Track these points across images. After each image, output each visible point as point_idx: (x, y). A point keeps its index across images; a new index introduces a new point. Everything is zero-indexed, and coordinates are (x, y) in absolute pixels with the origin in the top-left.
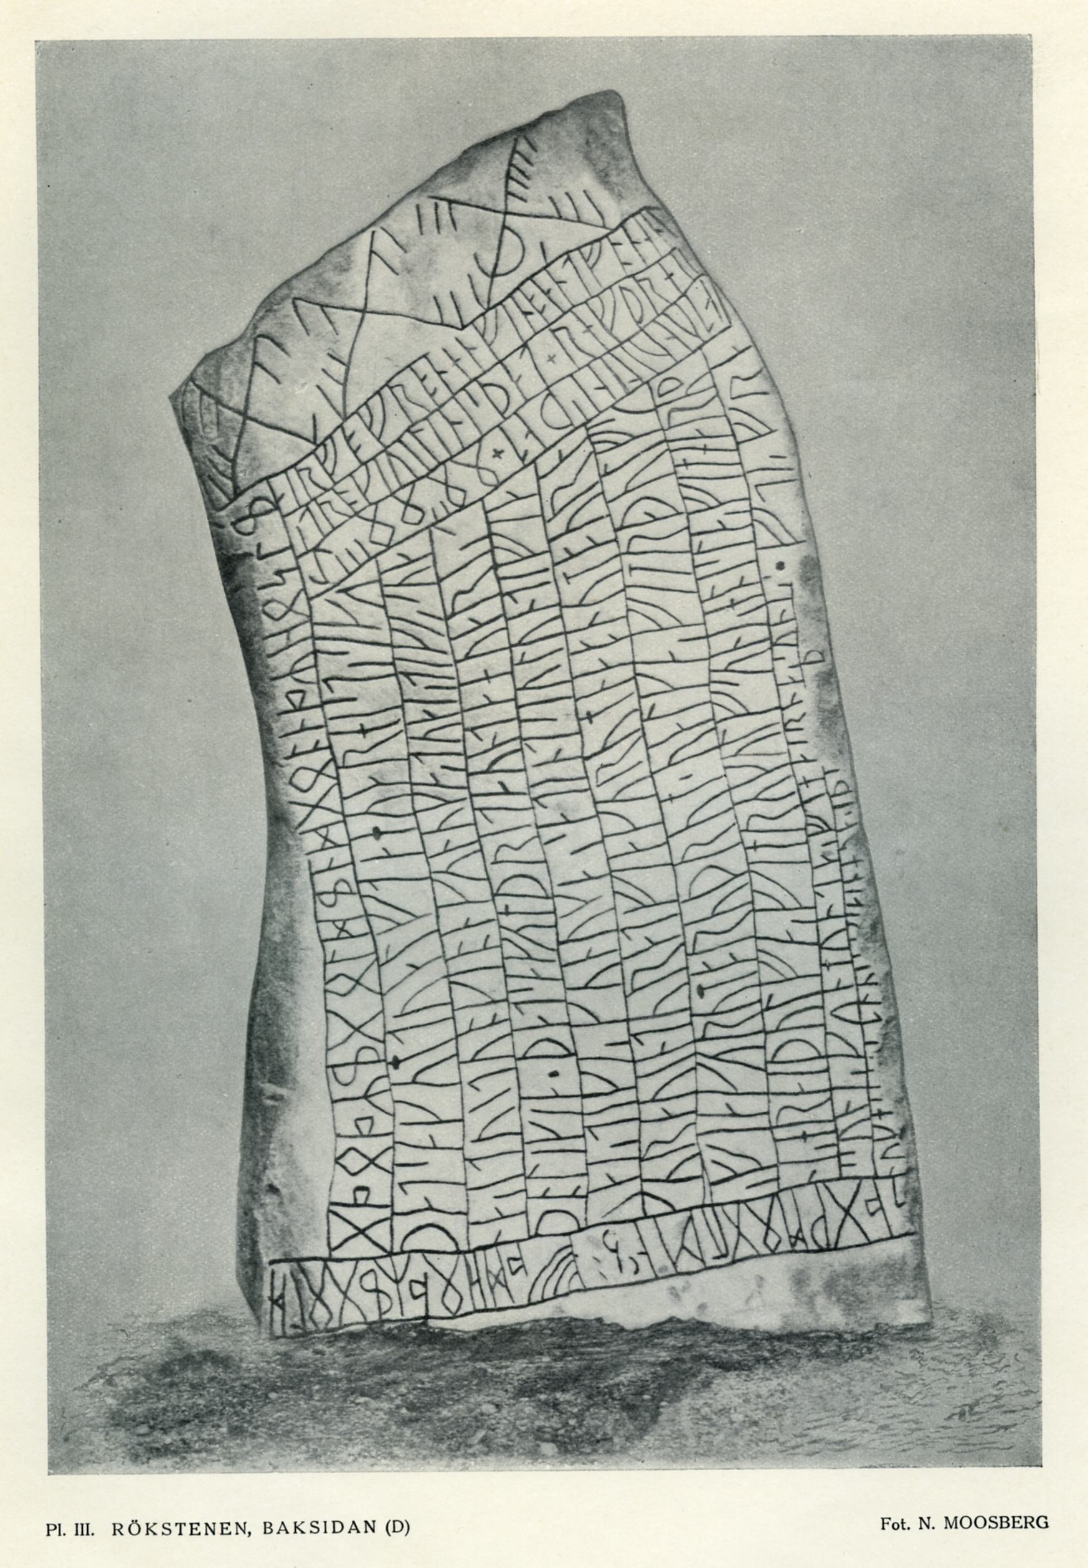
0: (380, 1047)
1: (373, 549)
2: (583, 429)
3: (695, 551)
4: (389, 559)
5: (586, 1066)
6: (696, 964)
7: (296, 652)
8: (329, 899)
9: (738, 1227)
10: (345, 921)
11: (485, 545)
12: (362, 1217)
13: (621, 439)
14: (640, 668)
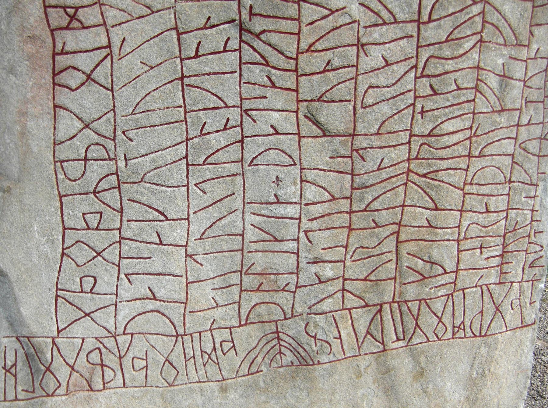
0: (110, 145)
5: (310, 175)
9: (416, 320)
10: (77, 9)
12: (88, 303)
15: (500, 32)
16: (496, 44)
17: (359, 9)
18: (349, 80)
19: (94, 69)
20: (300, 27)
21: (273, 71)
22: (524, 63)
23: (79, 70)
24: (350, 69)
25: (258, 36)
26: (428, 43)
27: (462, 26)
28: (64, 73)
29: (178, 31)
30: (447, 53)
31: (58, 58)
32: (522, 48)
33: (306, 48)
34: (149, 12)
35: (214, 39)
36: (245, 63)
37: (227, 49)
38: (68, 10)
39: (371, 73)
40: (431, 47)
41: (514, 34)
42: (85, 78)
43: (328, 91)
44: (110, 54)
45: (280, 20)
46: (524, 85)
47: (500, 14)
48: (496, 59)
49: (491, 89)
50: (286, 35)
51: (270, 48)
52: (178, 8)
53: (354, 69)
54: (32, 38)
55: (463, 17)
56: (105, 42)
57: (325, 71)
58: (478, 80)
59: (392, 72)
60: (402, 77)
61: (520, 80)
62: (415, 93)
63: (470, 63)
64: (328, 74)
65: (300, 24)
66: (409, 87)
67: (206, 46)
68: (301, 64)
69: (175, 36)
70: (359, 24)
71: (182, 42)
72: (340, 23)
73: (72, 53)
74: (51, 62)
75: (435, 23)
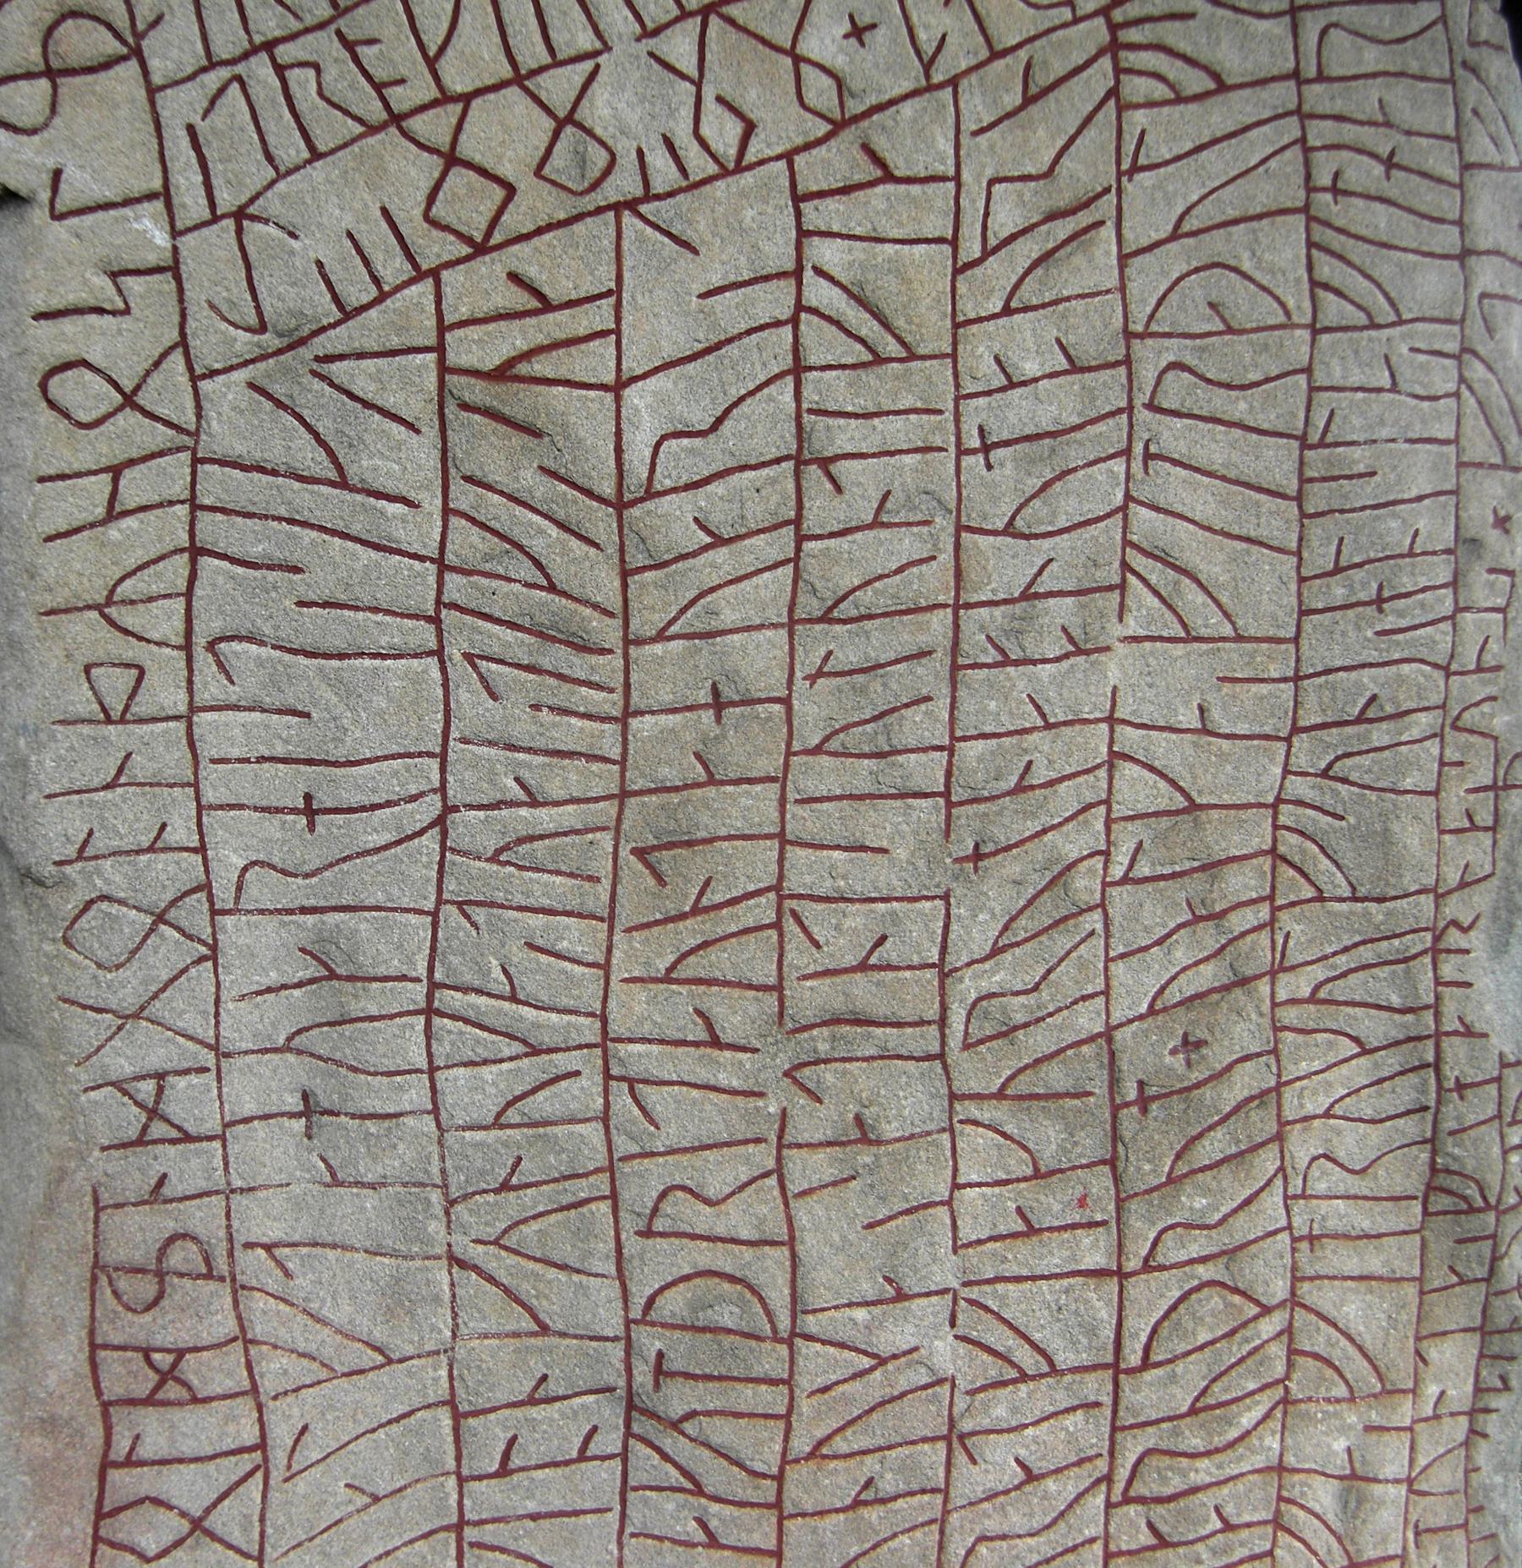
1: (435, 248)
2: (1100, 21)
3: (1314, 437)
4: (479, 286)
6: (1131, 1528)
7: (136, 537)
8: (146, 1288)
10: (180, 1354)
11: (775, 301)
13: (1196, 82)
14: (1128, 738)
15: (1336, 1369)
16: (1328, 1400)
17: (954, 1350)
18: (923, 1525)
19: (214, 1505)
20: (792, 1399)
21: (715, 1508)
22: (1406, 1437)
23: (171, 1508)
24: (926, 1497)
25: (676, 1425)
26: (1142, 1419)
27: (1233, 1373)
28: (129, 1513)
29: (454, 1408)
30: (1195, 1441)
31: (114, 1475)
32: (1397, 1398)
33: (808, 1449)
34: (380, 1359)
35: (555, 1430)
36: (635, 1489)
37: (589, 1453)
38: (157, 1356)
39: (986, 1505)
40: (1150, 1430)
41: (1376, 1368)
42: (186, 1526)
43: (864, 1553)
44: (265, 1466)
45: (739, 1386)
46: (1411, 1491)
47: (1335, 1326)
48: (1329, 1441)
49: (1317, 1516)
50: (754, 1421)
51: (707, 1453)
52: (460, 1353)
53: (939, 1498)
54: (50, 1425)
55: (1237, 1349)
56: (250, 1435)
57: (857, 1503)
58: (1280, 1498)
59: (1044, 1498)
60: (1070, 1506)
61: (1397, 1481)
62: (1106, 1546)
63: (1259, 1461)
64: (865, 1512)
65: (792, 1392)
66: (1088, 1533)
67: (533, 1449)
68: (792, 1491)
69: (447, 1422)
70: (953, 1386)
71: (466, 1436)
72: (903, 1384)
73: (154, 1463)
74: (95, 1483)
75: (1159, 1372)
